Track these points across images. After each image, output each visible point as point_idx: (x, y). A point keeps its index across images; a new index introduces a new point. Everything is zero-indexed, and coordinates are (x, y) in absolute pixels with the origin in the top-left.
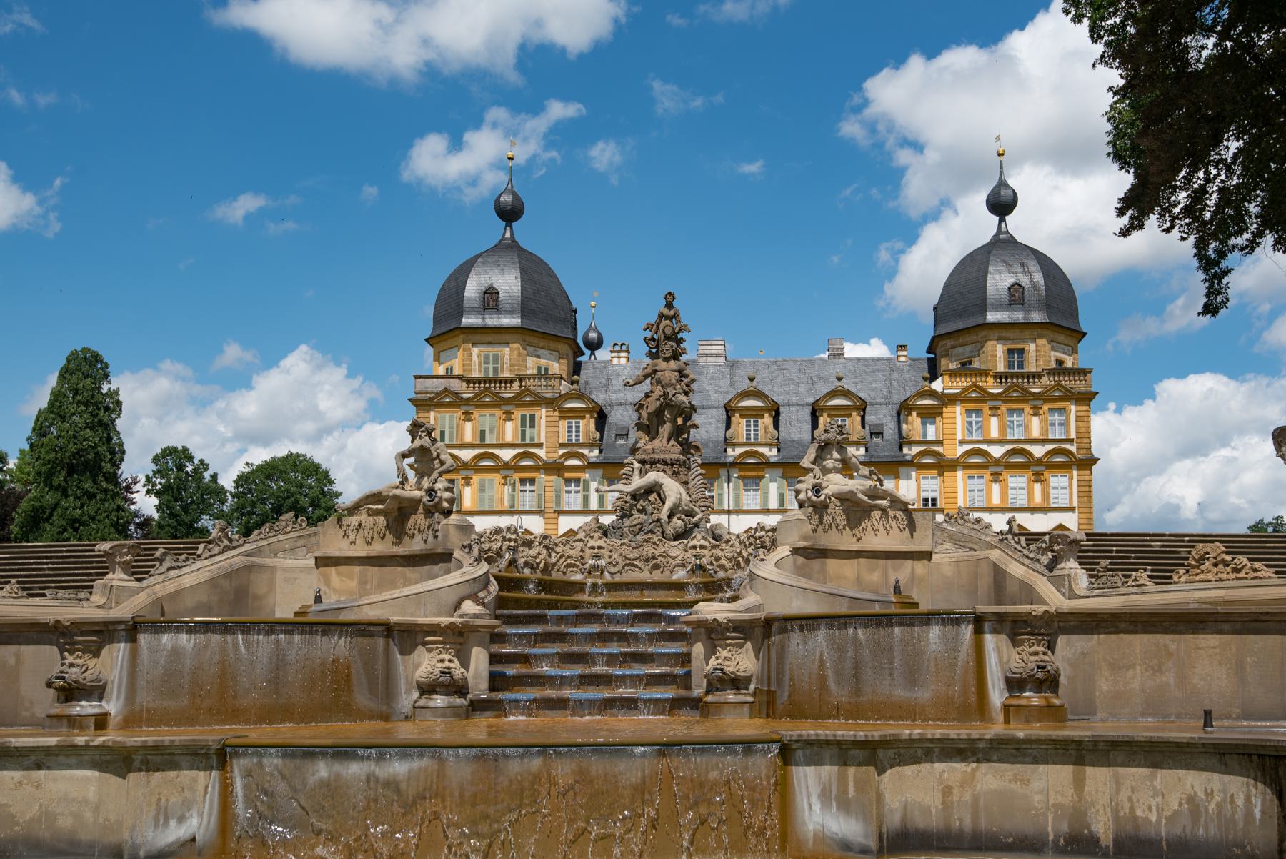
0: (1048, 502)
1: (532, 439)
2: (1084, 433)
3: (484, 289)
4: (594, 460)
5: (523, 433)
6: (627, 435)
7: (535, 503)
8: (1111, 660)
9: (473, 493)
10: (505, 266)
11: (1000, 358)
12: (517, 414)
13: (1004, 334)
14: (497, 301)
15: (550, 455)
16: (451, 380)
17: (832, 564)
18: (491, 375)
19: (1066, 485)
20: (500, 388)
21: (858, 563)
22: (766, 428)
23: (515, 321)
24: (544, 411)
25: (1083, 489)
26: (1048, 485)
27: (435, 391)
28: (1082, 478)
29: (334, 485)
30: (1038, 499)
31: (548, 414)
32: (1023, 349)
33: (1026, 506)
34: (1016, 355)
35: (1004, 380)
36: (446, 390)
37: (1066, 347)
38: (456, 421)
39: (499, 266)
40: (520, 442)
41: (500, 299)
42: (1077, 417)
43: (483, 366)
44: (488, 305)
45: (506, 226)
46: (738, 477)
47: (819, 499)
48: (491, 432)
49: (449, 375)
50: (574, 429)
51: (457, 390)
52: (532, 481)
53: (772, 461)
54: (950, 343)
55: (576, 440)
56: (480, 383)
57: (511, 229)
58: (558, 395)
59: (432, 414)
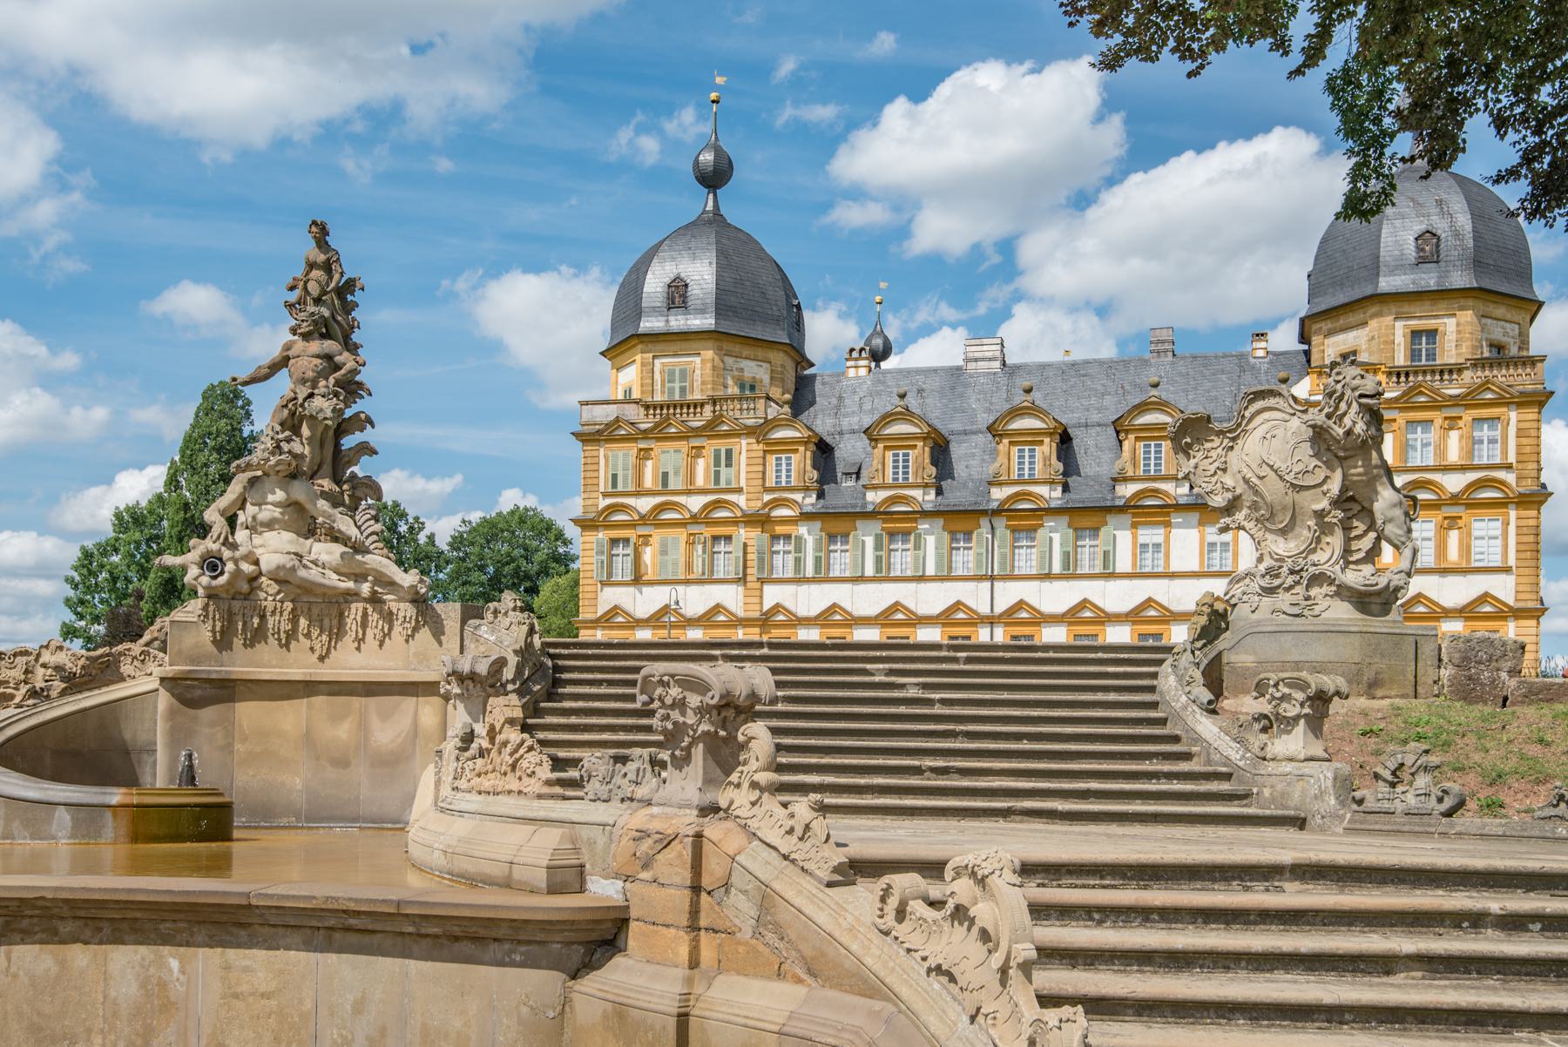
0: (1468, 560)
1: (728, 482)
2: (1532, 453)
3: (668, 280)
4: (809, 509)
5: (717, 474)
6: (858, 474)
7: (732, 568)
8: (35, 1019)
9: (653, 556)
10: (697, 248)
11: (1399, 345)
12: (711, 446)
13: (1406, 308)
14: (684, 297)
15: (752, 504)
16: (626, 406)
17: (248, 712)
18: (677, 398)
19: (1498, 533)
20: (688, 414)
21: (309, 707)
22: (1046, 460)
23: (707, 322)
24: (744, 442)
25: (1525, 539)
26: (1469, 534)
27: (605, 421)
28: (1524, 523)
29: (570, 546)
30: (1453, 554)
31: (750, 447)
32: (1436, 331)
33: (1433, 566)
34: (1424, 339)
35: (1403, 379)
36: (617, 419)
37: (1508, 325)
38: (632, 460)
39: (690, 248)
40: (713, 487)
41: (689, 294)
42: (1519, 430)
43: (667, 385)
44: (673, 303)
45: (709, 193)
46: (1007, 527)
47: (214, 583)
48: (676, 473)
49: (628, 401)
50: (784, 467)
51: (633, 419)
52: (728, 538)
53: (1052, 506)
54: (1326, 325)
55: (787, 482)
56: (662, 409)
57: (715, 196)
58: (762, 421)
59: (602, 450)
